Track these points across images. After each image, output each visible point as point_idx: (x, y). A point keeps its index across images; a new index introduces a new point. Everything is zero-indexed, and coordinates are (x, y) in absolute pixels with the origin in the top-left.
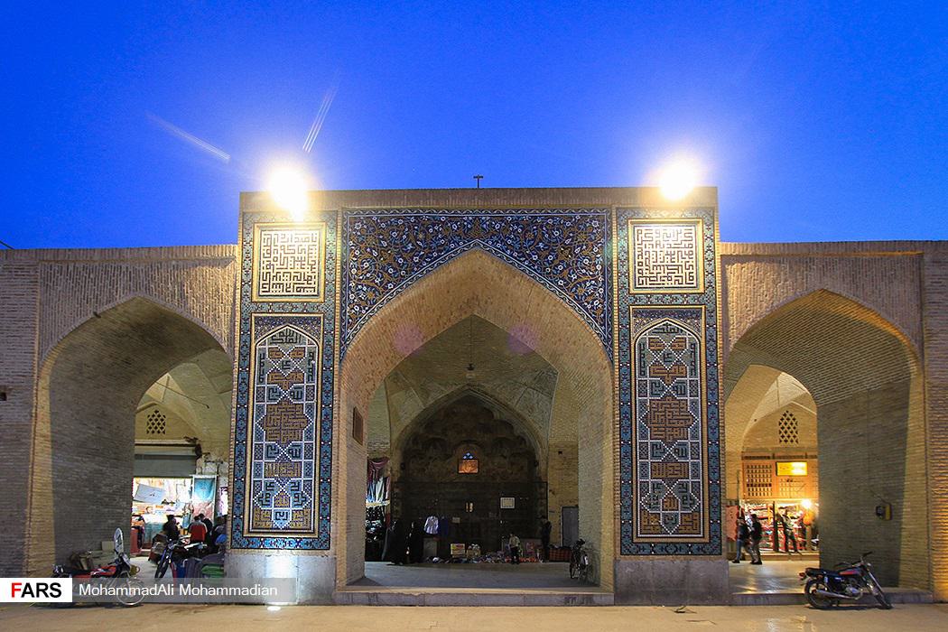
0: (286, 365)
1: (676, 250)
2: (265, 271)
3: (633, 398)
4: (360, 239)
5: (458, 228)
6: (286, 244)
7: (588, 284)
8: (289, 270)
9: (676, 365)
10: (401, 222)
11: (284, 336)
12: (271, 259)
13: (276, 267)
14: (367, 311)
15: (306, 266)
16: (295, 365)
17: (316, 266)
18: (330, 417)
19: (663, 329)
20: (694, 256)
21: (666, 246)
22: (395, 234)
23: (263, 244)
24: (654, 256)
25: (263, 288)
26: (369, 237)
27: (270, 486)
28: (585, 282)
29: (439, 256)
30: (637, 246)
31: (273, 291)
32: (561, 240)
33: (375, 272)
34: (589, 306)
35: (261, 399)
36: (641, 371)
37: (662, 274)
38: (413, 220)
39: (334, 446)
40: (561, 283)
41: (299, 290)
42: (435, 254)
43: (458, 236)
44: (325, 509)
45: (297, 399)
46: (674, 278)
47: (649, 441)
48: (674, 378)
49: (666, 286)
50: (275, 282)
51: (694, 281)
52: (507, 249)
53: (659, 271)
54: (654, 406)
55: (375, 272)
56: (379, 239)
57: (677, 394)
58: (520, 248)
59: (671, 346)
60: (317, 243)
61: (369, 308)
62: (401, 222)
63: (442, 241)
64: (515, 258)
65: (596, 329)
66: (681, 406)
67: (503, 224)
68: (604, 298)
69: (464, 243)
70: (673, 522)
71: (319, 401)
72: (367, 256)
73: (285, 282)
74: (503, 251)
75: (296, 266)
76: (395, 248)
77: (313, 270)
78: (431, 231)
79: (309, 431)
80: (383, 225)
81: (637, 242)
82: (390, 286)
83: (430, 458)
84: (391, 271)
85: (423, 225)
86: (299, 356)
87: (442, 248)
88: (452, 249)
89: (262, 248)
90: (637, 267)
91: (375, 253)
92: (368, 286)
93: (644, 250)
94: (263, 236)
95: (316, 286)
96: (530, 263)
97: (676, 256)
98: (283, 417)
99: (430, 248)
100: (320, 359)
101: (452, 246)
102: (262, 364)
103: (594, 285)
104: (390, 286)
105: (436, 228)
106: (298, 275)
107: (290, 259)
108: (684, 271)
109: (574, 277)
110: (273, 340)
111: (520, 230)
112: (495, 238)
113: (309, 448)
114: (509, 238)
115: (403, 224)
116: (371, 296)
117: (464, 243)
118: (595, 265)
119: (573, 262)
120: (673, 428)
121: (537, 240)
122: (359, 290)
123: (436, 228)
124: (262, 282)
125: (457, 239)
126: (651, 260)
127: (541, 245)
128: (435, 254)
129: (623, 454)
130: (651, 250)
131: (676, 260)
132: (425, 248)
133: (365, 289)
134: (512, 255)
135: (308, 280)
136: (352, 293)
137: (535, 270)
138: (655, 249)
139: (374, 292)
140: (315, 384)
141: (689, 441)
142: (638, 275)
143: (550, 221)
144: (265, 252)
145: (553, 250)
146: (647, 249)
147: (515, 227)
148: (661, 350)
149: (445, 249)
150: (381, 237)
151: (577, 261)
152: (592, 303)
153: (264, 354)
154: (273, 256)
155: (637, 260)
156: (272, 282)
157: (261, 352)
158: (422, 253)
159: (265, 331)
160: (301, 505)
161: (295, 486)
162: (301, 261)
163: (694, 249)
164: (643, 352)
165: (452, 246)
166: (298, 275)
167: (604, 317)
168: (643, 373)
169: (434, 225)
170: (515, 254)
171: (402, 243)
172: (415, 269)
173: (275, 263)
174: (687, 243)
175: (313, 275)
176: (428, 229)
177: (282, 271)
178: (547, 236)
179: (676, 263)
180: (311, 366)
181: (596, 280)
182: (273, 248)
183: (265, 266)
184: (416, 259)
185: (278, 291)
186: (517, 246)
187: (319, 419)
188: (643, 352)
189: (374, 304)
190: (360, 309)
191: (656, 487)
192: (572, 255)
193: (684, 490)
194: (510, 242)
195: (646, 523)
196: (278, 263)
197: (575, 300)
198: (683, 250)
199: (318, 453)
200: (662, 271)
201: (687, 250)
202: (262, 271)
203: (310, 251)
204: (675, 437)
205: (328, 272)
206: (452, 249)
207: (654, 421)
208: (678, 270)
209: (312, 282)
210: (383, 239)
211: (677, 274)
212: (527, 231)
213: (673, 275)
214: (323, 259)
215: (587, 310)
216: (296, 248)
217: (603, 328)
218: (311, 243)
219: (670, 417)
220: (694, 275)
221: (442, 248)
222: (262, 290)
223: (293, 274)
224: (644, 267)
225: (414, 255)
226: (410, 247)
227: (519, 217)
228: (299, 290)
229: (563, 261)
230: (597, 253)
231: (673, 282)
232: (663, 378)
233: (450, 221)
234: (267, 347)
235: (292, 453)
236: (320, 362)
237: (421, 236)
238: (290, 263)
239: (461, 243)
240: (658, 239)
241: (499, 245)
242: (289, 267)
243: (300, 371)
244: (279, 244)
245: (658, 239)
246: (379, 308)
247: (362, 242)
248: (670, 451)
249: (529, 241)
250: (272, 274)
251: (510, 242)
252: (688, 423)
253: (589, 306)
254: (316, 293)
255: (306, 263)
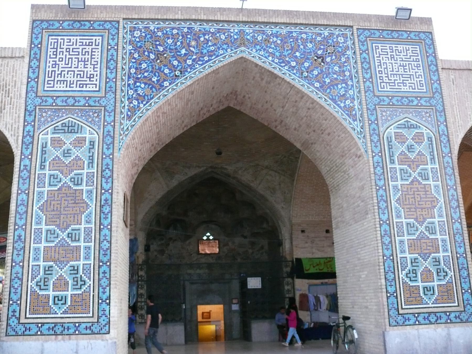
0: (67, 153)
1: (407, 63)
2: (51, 69)
3: (387, 183)
4: (139, 44)
5: (226, 38)
6: (71, 47)
7: (340, 86)
8: (73, 69)
9: (418, 154)
10: (175, 31)
11: (65, 126)
12: (57, 60)
13: (61, 66)
14: (144, 105)
15: (89, 66)
16: (75, 152)
17: (99, 66)
18: (109, 202)
19: (405, 125)
20: (421, 68)
21: (399, 59)
22: (170, 41)
23: (49, 47)
24: (391, 67)
25: (48, 84)
26: (147, 43)
27: (48, 270)
28: (337, 85)
29: (209, 60)
30: (376, 59)
31: (58, 87)
32: (314, 51)
33: (152, 72)
34: (342, 105)
35: (41, 185)
36: (391, 160)
37: (399, 81)
38: (185, 30)
39: (113, 229)
40: (317, 85)
41: (81, 86)
42: (206, 58)
43: (226, 44)
44: (104, 293)
45: (78, 184)
46: (408, 85)
47: (404, 220)
48: (418, 166)
49: (403, 90)
50: (59, 79)
51: (424, 88)
52: (269, 56)
53: (396, 78)
54: (405, 190)
55: (152, 72)
56: (156, 45)
57: (423, 179)
58: (280, 56)
59: (412, 139)
60: (100, 47)
61: (147, 102)
62: (175, 31)
63: (212, 48)
64: (276, 63)
65: (351, 124)
66: (426, 189)
67: (264, 37)
68: (354, 99)
69: (232, 50)
70: (432, 292)
71: (99, 187)
72: (144, 58)
73: (69, 79)
74: (266, 57)
75: (80, 66)
76: (171, 52)
77: (95, 69)
78: (202, 39)
79: (89, 215)
80: (160, 34)
81: (375, 56)
82: (166, 84)
83: (171, 239)
84: (167, 71)
85: (195, 35)
86: (81, 145)
87: (212, 54)
88: (221, 55)
89: (49, 50)
90: (378, 75)
91: (152, 56)
92: (145, 84)
93: (382, 62)
94: (50, 41)
95: (98, 83)
96: (289, 68)
97: (407, 67)
98: (63, 202)
99: (202, 53)
100: (101, 147)
101: (221, 52)
102: (44, 153)
103: (344, 87)
104: (166, 84)
105: (207, 37)
106: (82, 73)
107: (74, 60)
108: (415, 79)
109: (328, 80)
110: (56, 131)
111: (279, 42)
112: (258, 47)
113: (88, 232)
114: (270, 48)
115: (178, 33)
116: (148, 91)
117: (232, 50)
118: (344, 71)
119: (326, 68)
120: (422, 209)
121: (294, 50)
122: (137, 87)
123: (207, 37)
124: (47, 79)
125: (225, 46)
126: (389, 70)
127: (298, 54)
128: (206, 58)
129: (383, 233)
130: (387, 62)
131: (408, 70)
132: (197, 53)
133: (143, 86)
134: (273, 61)
135: (90, 78)
136: (131, 89)
137: (294, 74)
138: (390, 61)
139: (151, 89)
140: (95, 171)
141: (436, 220)
142: (379, 81)
143: (304, 36)
144: (52, 53)
145: (308, 59)
146: (384, 61)
147: (275, 39)
148: (405, 142)
149: (215, 54)
150: (158, 43)
151: (329, 68)
152: (345, 103)
153: (46, 143)
154: (58, 57)
155: (377, 70)
156: (56, 79)
157: (44, 141)
158: (194, 57)
159: (48, 122)
160: (81, 288)
161: (74, 270)
162: (85, 61)
163: (420, 63)
164: (390, 143)
165: (221, 52)
166: (82, 73)
167: (356, 114)
168: (392, 162)
169: (204, 35)
170: (276, 61)
171: (176, 49)
172: (189, 70)
173: (60, 63)
174: (415, 58)
175: (95, 73)
176: (199, 38)
177: (66, 70)
178: (302, 47)
179: (408, 73)
180: (91, 154)
181: (346, 84)
182: (59, 50)
183: (51, 65)
184: (189, 62)
185: (62, 87)
186: (278, 54)
187: (98, 204)
188: (390, 143)
189: (152, 98)
190: (139, 103)
191: (414, 261)
192: (324, 63)
193: (438, 263)
194: (271, 50)
195: (408, 296)
196: (63, 62)
197: (330, 99)
198: (413, 63)
199: (98, 236)
200: (398, 78)
201: (416, 63)
202: (47, 69)
203: (93, 53)
204: (425, 217)
205: (109, 71)
206: (221, 55)
207: (405, 203)
208: (410, 77)
209: (94, 79)
210: (160, 45)
211: (410, 82)
212: (285, 43)
213: (407, 82)
214: (104, 61)
215: (340, 107)
216: (80, 50)
217: (356, 123)
218: (94, 46)
219: (419, 199)
220: (423, 82)
221: (212, 54)
222: (46, 85)
223: (76, 73)
224: (384, 75)
225: (187, 59)
226: (183, 51)
227: (277, 32)
228: (81, 86)
229: (317, 68)
230: (345, 62)
231: (408, 87)
232: (409, 166)
233: (219, 32)
234: (49, 136)
235: (71, 237)
236: (100, 151)
237: (193, 43)
238: (74, 63)
239: (229, 50)
240: (392, 53)
241: (262, 53)
242: (73, 66)
243: (80, 159)
244: (65, 47)
245: (392, 53)
246: (155, 103)
247: (140, 47)
248: (422, 229)
249: (287, 50)
250: (57, 72)
251: (271, 50)
252: (434, 204)
253: (342, 105)
254: (97, 89)
255: (89, 63)
